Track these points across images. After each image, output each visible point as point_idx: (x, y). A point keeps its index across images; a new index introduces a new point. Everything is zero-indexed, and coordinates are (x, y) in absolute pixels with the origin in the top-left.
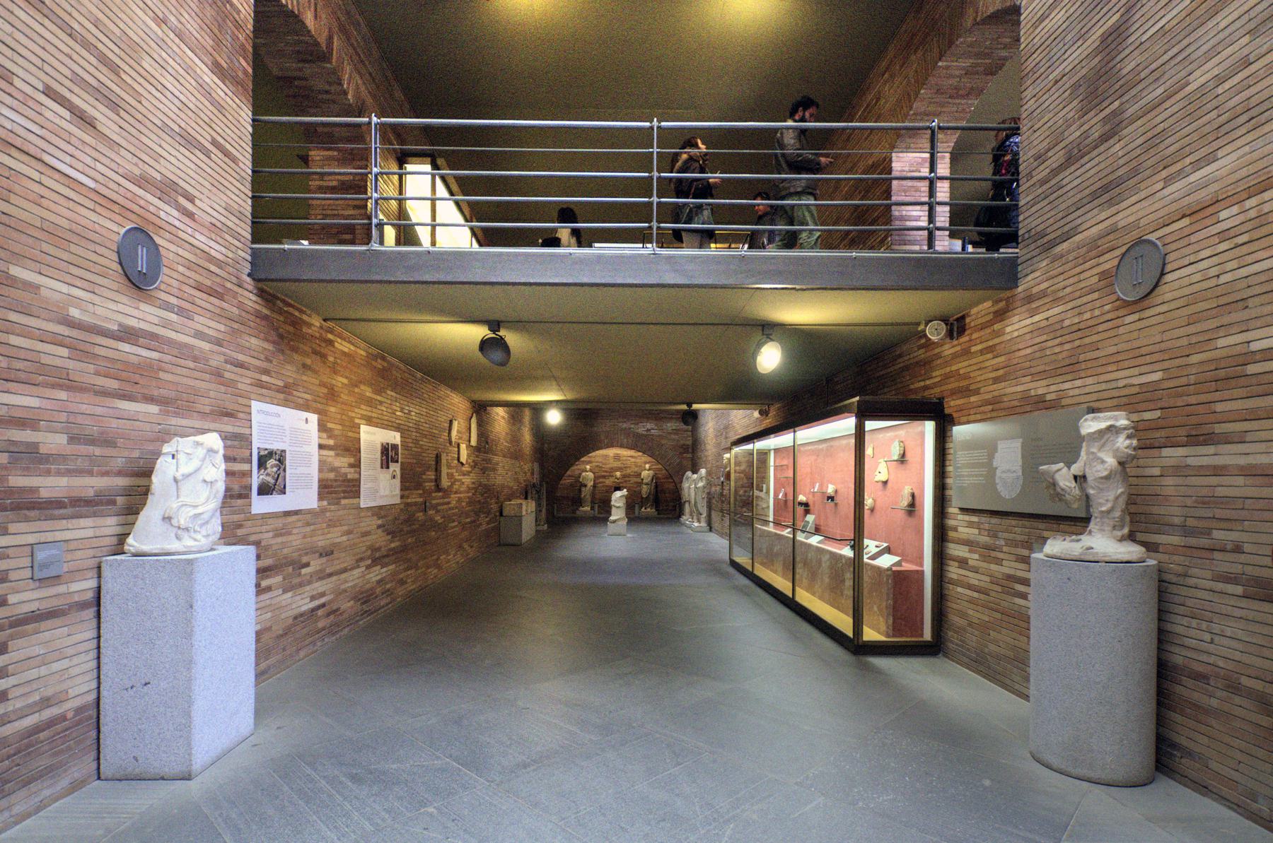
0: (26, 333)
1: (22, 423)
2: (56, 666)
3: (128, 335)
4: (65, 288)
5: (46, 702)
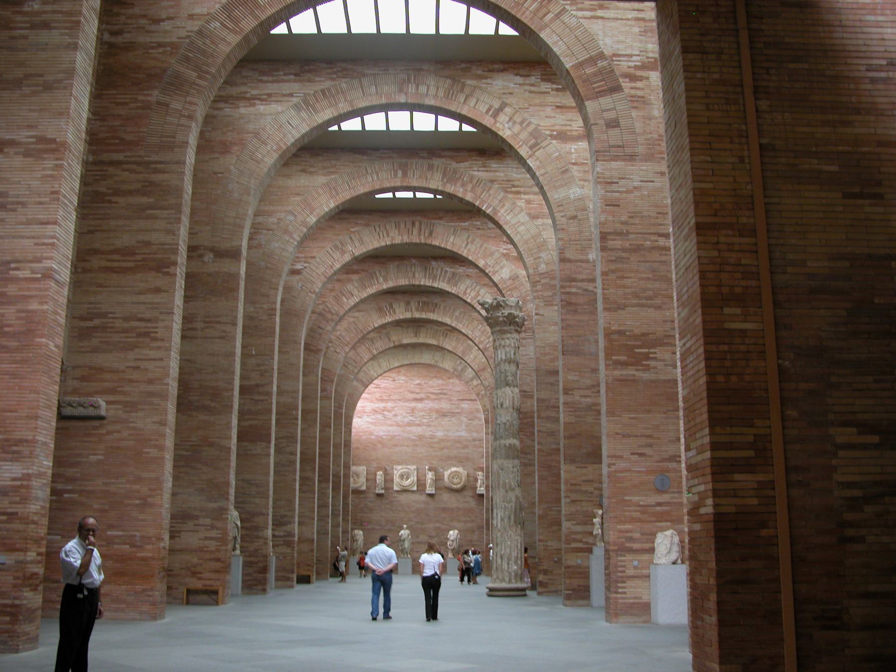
0: (629, 511)
1: (627, 531)
2: (639, 590)
3: (659, 504)
4: (638, 498)
5: (636, 598)
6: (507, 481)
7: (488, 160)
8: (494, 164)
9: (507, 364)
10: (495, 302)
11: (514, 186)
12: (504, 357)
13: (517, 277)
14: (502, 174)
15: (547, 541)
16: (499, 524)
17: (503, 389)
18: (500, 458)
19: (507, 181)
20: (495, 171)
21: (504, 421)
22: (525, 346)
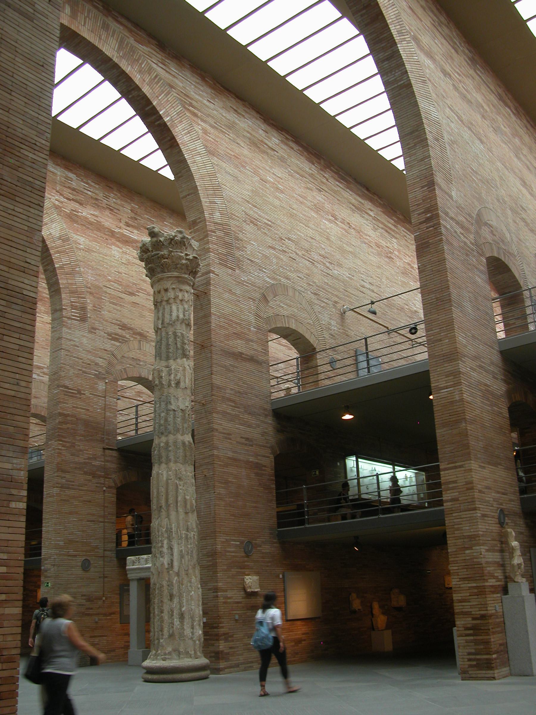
6: (188, 497)
7: (168, 59)
8: (173, 68)
9: (184, 326)
10: (180, 236)
11: (191, 105)
12: (181, 316)
13: (68, 239)
14: (181, 85)
15: (226, 591)
16: (176, 564)
17: (179, 361)
18: (176, 462)
19: (185, 95)
20: (174, 76)
21: (182, 407)
22: (70, 329)
